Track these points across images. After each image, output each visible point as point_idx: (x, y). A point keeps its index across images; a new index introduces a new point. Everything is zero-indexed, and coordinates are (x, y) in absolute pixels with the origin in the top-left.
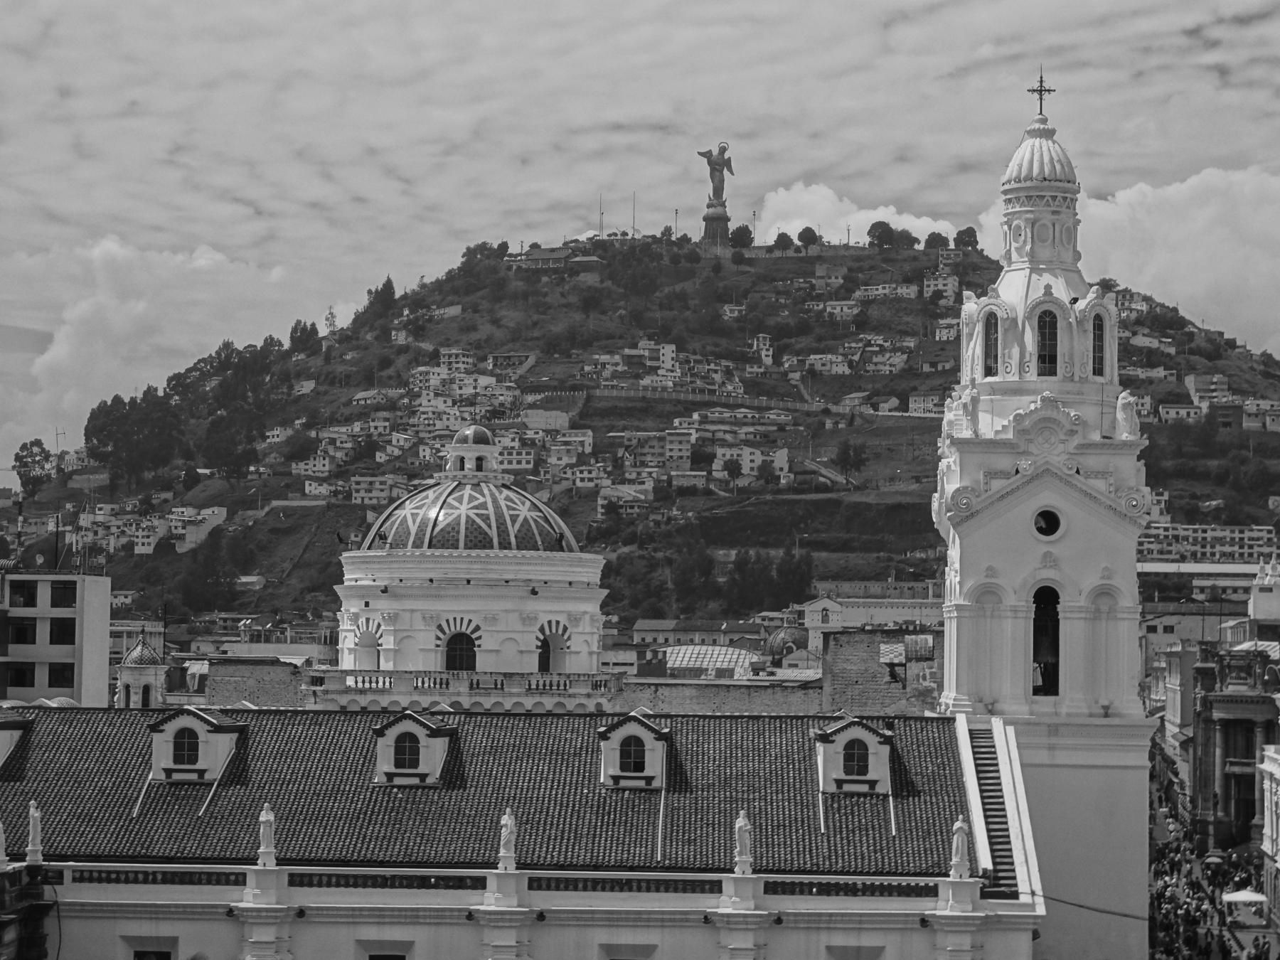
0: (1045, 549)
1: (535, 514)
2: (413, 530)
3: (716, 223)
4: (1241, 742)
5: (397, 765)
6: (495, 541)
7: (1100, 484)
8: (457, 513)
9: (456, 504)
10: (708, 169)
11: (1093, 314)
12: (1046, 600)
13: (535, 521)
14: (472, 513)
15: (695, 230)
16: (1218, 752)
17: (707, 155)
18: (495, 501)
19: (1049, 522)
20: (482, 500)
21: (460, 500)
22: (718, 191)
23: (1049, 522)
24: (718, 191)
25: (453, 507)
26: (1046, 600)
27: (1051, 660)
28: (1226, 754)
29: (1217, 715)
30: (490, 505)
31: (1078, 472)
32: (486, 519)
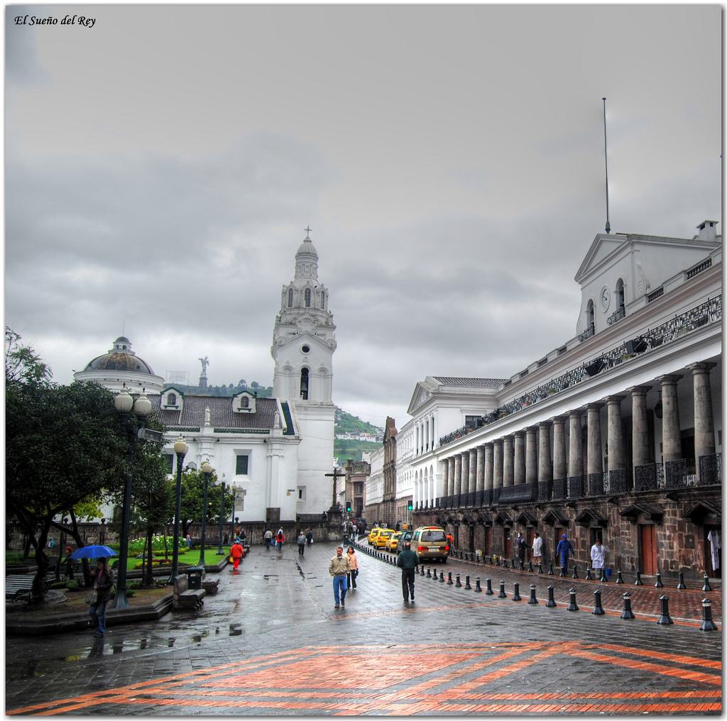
0: (305, 356)
3: (203, 379)
4: (359, 488)
7: (322, 338)
10: (201, 364)
12: (305, 372)
15: (196, 383)
16: (353, 492)
17: (201, 360)
19: (306, 349)
22: (204, 370)
23: (306, 349)
24: (204, 370)
26: (305, 372)
28: (355, 492)
29: (352, 481)
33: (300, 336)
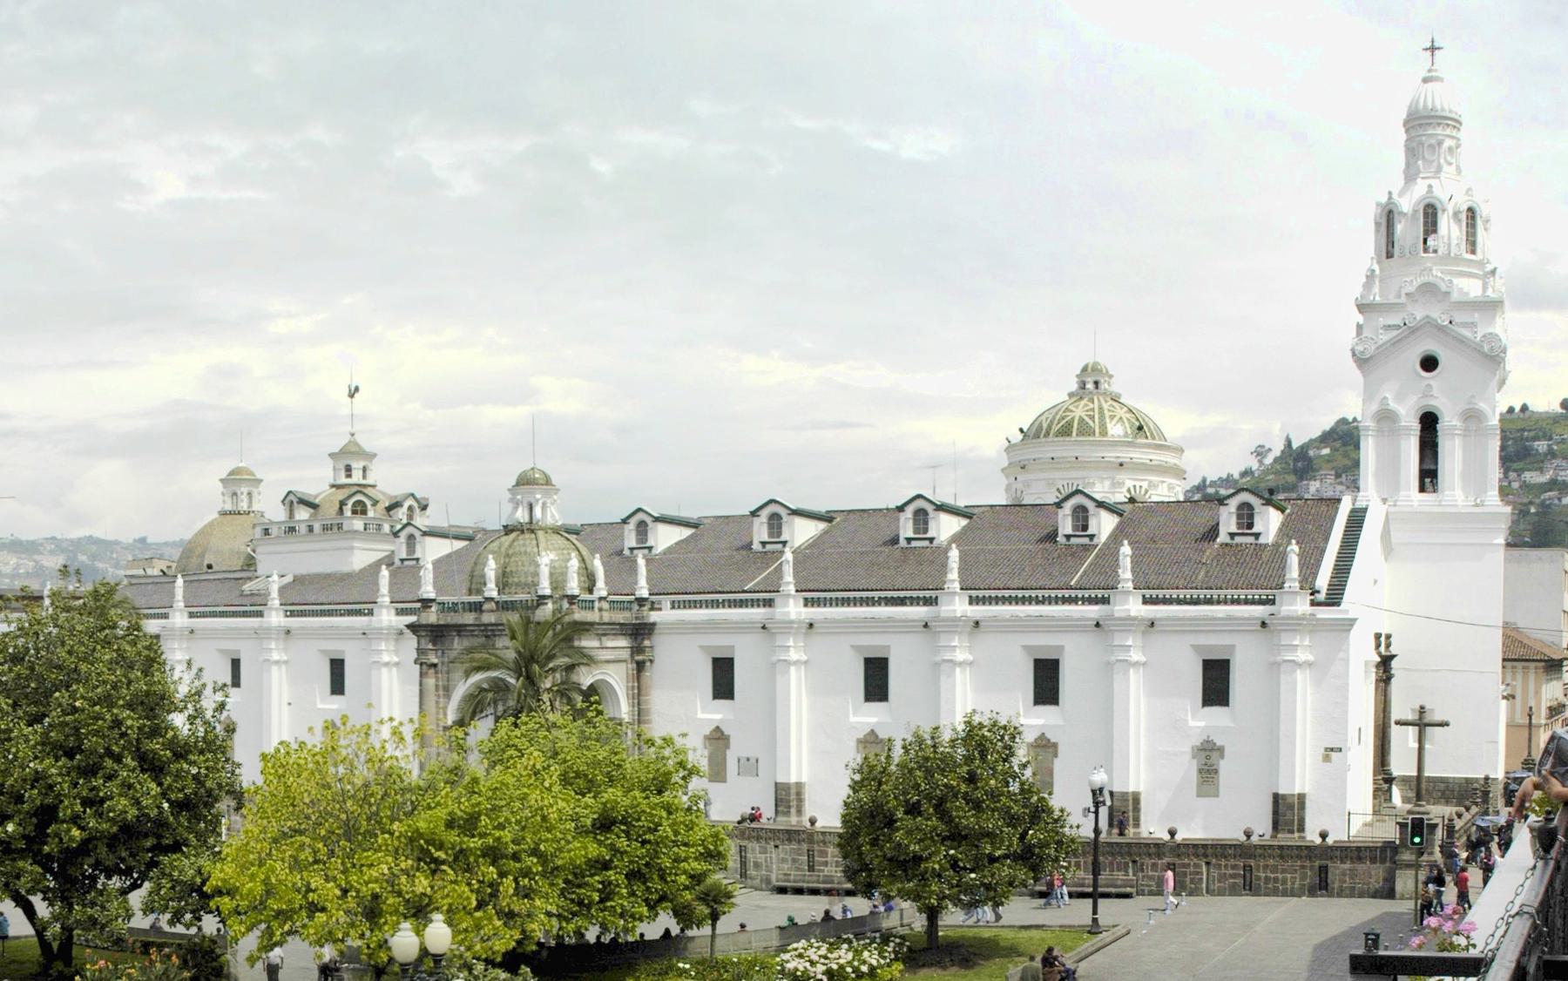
1: (1129, 415)
2: (1045, 426)
5: (915, 533)
6: (1097, 431)
8: (1072, 415)
9: (1074, 409)
11: (1466, 208)
12: (1429, 422)
13: (1128, 420)
14: (1083, 415)
18: (1101, 408)
20: (1091, 406)
21: (1077, 407)
23: (1429, 363)
25: (1071, 411)
26: (1429, 422)
27: (1432, 467)
30: (1096, 411)
31: (1451, 322)
32: (1092, 418)
33: (1414, 331)
